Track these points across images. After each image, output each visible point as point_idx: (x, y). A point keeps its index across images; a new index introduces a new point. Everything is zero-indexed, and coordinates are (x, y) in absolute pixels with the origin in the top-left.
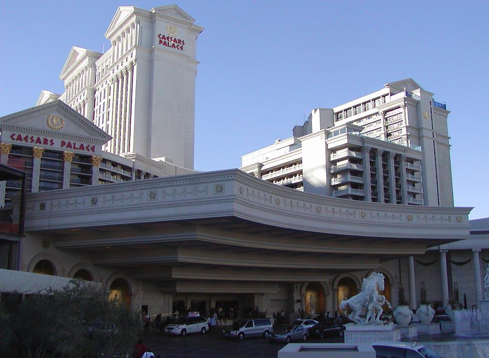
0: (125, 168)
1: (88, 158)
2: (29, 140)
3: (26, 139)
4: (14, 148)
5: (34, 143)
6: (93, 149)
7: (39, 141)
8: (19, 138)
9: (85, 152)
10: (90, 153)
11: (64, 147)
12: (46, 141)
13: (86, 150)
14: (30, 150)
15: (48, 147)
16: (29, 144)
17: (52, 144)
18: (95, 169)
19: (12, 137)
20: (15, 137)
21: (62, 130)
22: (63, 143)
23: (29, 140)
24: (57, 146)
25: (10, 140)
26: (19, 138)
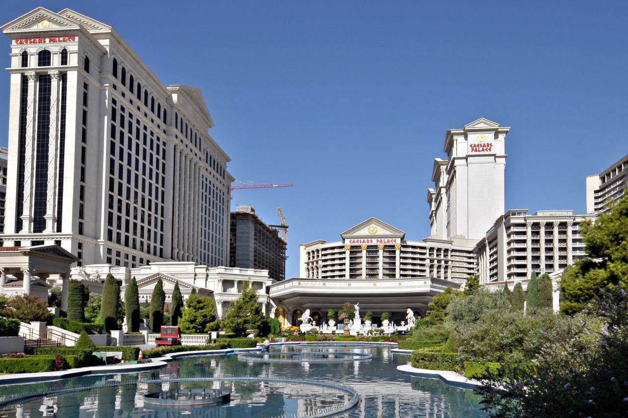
0: (421, 248)
1: (393, 246)
2: (359, 242)
3: (357, 242)
4: (352, 247)
5: (362, 243)
6: (395, 241)
7: (364, 242)
8: (354, 242)
9: (391, 243)
10: (394, 243)
11: (379, 243)
12: (368, 241)
13: (391, 243)
14: (360, 247)
15: (370, 244)
16: (359, 244)
17: (372, 242)
18: (398, 252)
19: (350, 242)
20: (352, 242)
21: (376, 234)
22: (378, 241)
23: (359, 242)
24: (374, 242)
25: (349, 243)
26: (354, 242)
